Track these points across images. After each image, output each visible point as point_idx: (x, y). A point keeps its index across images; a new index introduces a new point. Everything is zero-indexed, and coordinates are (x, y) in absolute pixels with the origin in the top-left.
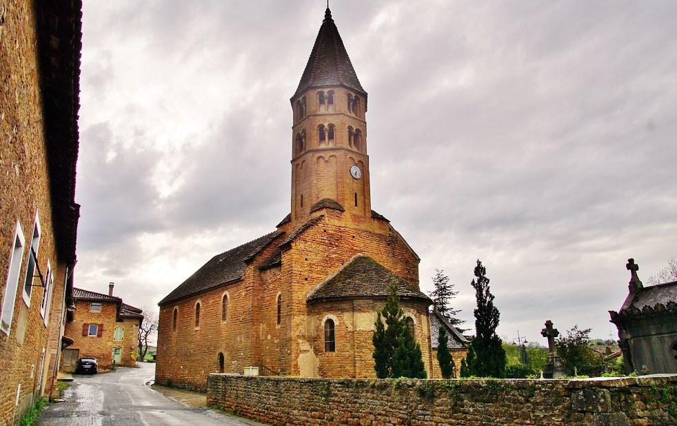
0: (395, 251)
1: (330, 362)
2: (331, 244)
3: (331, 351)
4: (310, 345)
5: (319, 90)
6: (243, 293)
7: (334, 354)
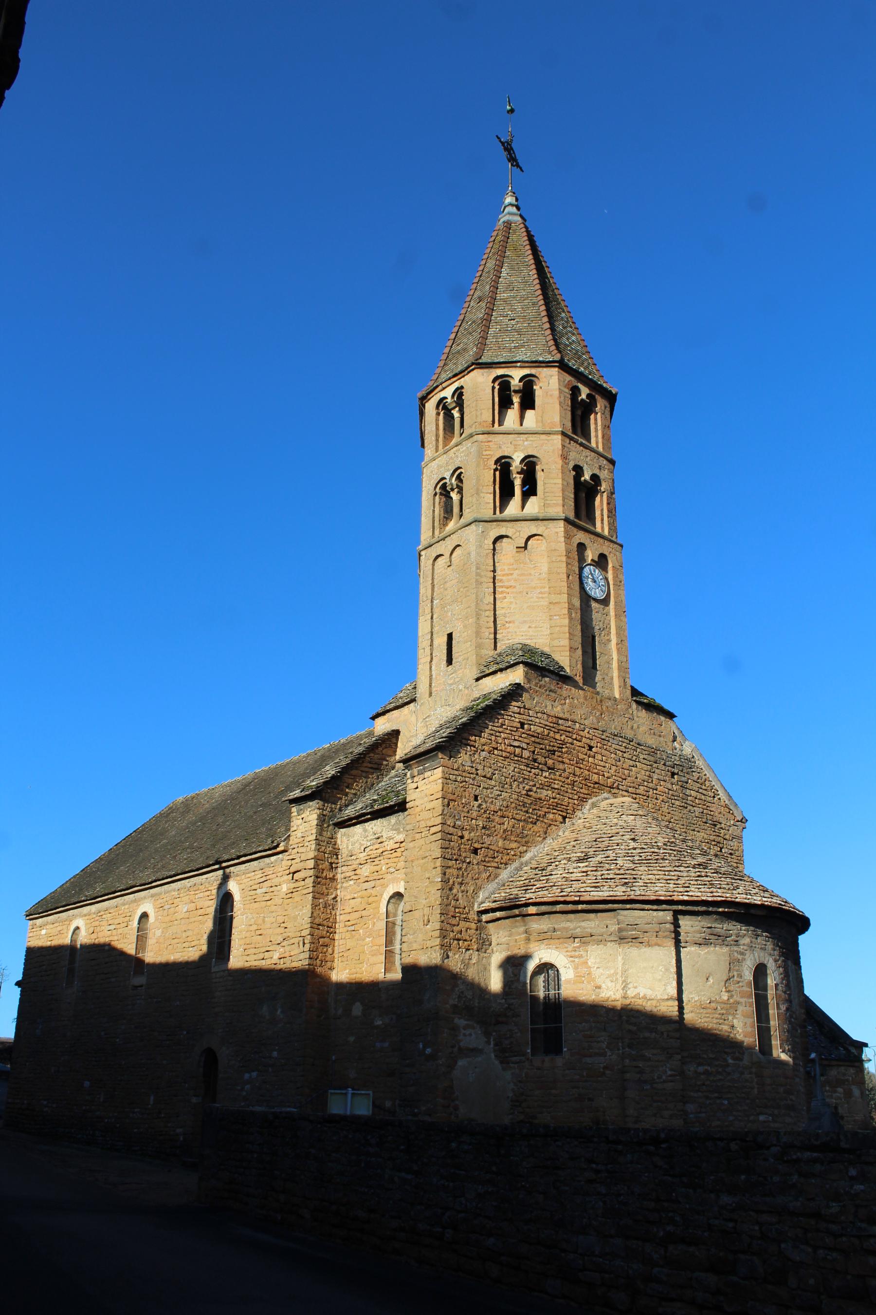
0: (688, 792)
2: (535, 760)
3: (547, 1052)
4: (487, 1034)
5: (500, 372)
6: (285, 888)
7: (559, 1061)
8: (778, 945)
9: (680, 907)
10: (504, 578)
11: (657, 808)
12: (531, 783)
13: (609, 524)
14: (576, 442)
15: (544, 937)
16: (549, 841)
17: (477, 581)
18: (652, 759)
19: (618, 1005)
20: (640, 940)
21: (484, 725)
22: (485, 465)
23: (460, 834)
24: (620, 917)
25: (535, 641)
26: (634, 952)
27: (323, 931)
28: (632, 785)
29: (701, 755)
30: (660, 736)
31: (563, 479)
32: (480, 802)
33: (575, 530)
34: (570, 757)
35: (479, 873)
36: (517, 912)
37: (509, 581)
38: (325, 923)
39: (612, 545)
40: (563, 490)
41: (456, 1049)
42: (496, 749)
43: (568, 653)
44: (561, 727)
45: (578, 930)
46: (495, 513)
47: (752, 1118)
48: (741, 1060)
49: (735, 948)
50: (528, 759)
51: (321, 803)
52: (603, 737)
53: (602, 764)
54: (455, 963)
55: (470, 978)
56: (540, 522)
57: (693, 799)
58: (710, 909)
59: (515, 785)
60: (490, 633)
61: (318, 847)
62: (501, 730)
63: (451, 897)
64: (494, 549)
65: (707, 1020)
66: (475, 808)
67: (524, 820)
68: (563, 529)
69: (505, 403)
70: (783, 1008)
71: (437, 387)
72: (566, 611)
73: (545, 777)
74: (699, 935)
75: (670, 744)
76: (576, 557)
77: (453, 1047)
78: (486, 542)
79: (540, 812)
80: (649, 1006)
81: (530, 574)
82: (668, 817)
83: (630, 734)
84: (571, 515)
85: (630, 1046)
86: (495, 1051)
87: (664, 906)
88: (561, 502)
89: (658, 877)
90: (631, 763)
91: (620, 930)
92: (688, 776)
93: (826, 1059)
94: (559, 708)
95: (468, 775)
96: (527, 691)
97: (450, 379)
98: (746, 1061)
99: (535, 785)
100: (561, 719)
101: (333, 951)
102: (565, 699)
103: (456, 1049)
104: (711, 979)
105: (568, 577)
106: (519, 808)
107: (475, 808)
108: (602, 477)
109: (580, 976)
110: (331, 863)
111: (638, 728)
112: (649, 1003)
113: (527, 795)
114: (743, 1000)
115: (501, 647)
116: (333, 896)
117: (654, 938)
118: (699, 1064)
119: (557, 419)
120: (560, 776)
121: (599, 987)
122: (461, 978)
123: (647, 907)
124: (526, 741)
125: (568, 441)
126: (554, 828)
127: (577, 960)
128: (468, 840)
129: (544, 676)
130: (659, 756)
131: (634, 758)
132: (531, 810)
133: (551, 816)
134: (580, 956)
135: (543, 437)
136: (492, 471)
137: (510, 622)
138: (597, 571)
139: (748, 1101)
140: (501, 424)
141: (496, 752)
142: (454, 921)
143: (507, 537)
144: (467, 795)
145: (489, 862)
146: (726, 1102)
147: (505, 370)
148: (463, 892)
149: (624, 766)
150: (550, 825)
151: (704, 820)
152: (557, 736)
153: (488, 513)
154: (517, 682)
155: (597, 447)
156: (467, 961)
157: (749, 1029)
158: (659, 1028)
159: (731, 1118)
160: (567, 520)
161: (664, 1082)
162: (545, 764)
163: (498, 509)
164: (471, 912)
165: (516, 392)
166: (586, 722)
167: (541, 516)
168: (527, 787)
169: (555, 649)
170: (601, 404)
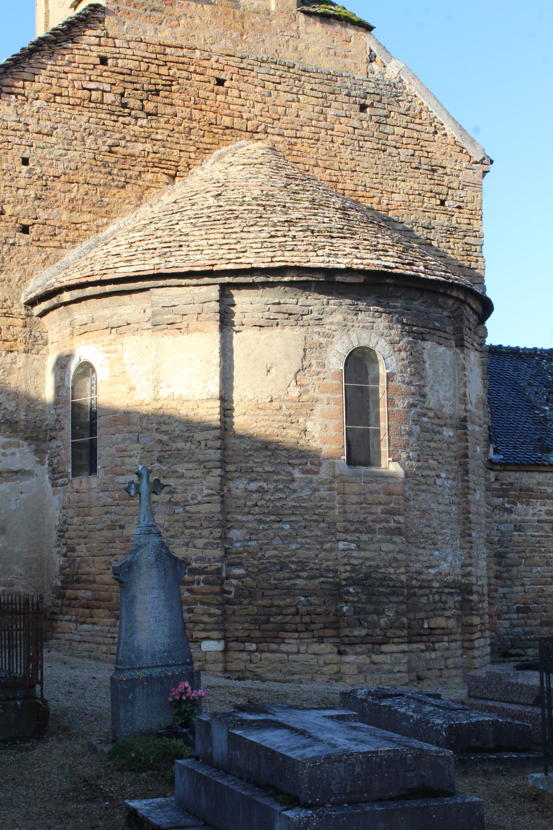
0: (389, 129)
1: (83, 510)
2: (124, 106)
7: (94, 481)
9: (227, 280)
11: (333, 154)
12: (118, 136)
16: (143, 209)
18: (327, 89)
19: (150, 408)
21: (39, 65)
24: (155, 298)
26: (170, 342)
28: (290, 126)
29: (415, 77)
30: (346, 57)
32: (31, 165)
35: (29, 256)
36: (54, 301)
42: (60, 95)
44: (169, 58)
45: (115, 318)
47: (327, 546)
49: (316, 329)
52: (242, 66)
53: (240, 101)
55: (12, 386)
57: (397, 138)
59: (89, 140)
62: (67, 69)
66: (23, 174)
67: (105, 184)
70: (401, 404)
73: (141, 127)
74: (260, 315)
75: (363, 67)
79: (122, 174)
80: (185, 411)
82: (351, 165)
83: (289, 57)
85: (159, 461)
86: (49, 472)
87: (206, 280)
89: (210, 242)
90: (290, 97)
91: (154, 314)
92: (390, 108)
94: (166, 32)
95: (13, 133)
96: (113, 13)
98: (324, 473)
99: (124, 138)
100: (169, 46)
102: (178, 19)
104: (273, 371)
106: (95, 169)
107: (23, 174)
109: (115, 376)
111: (307, 48)
113: (110, 152)
114: (324, 396)
118: (251, 480)
120: (167, 122)
121: (132, 389)
123: (184, 281)
124: (109, 80)
126: (154, 191)
127: (112, 355)
128: (11, 216)
131: (295, 90)
132: (115, 171)
133: (149, 176)
134: (116, 351)
139: (322, 525)
141: (58, 99)
144: (10, 157)
145: (45, 241)
146: (287, 527)
149: (277, 102)
150: (148, 187)
151: (414, 165)
152: (163, 70)
154: (101, 3)
156: (8, 366)
157: (332, 433)
158: (196, 436)
159: (294, 547)
161: (199, 503)
162: (142, 109)
166: (214, 48)
168: (110, 142)
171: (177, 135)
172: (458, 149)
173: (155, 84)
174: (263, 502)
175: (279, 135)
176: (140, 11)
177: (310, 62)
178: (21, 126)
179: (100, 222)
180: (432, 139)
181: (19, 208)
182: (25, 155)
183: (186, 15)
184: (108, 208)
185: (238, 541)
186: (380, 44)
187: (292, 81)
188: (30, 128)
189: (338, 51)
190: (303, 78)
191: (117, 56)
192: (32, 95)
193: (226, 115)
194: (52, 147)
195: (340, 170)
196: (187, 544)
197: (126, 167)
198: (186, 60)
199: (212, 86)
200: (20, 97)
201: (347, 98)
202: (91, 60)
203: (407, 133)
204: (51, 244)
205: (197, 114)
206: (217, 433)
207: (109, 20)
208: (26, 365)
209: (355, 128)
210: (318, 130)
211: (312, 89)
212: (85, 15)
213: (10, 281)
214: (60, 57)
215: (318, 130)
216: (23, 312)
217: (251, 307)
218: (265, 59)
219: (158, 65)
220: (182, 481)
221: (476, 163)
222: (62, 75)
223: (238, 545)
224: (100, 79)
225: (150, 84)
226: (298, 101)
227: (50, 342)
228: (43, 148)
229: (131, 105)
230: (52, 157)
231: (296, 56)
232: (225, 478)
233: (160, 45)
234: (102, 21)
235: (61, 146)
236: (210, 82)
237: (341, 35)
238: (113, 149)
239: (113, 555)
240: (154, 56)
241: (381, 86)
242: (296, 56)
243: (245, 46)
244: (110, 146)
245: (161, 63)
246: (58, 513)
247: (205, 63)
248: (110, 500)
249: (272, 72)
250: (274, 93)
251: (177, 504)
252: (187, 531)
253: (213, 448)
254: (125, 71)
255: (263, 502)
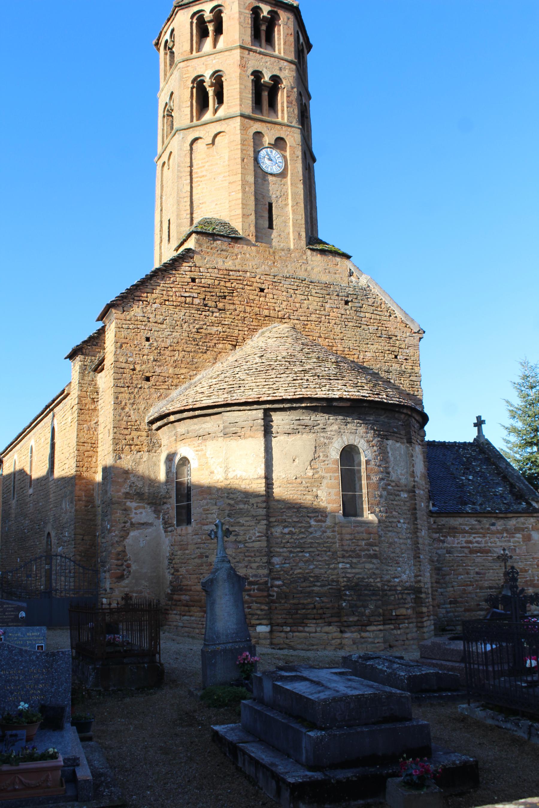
0: (362, 315)
1: (183, 547)
2: (206, 305)
4: (157, 512)
5: (196, 9)
7: (190, 529)
8: (372, 429)
9: (268, 406)
10: (199, 170)
11: (329, 330)
12: (202, 323)
13: (288, 113)
14: (255, 52)
15: (183, 438)
17: (178, 176)
18: (325, 292)
20: (238, 434)
21: (156, 284)
22: (185, 86)
23: (132, 367)
24: (225, 418)
25: (219, 215)
26: (234, 444)
27: (88, 447)
28: (303, 314)
30: (335, 273)
31: (240, 84)
32: (151, 341)
33: (251, 122)
34: (240, 299)
35: (150, 395)
36: (165, 421)
37: (202, 172)
38: (89, 441)
39: (289, 129)
40: (241, 93)
41: (128, 524)
42: (168, 300)
43: (241, 220)
44: (232, 277)
45: (202, 430)
46: (192, 121)
47: (332, 566)
48: (325, 522)
49: (322, 434)
50: (198, 305)
51: (82, 357)
52: (274, 280)
53: (273, 301)
54: (127, 462)
55: (140, 472)
56: (223, 122)
57: (368, 319)
58: (294, 405)
59: (185, 326)
60: (187, 214)
61: (81, 388)
62: (172, 286)
63: (123, 414)
64: (191, 149)
65: (293, 492)
66: (147, 347)
67: (195, 351)
68: (239, 124)
69: (203, 33)
70: (375, 479)
71: (161, 33)
72: (240, 187)
73: (216, 317)
74: (288, 427)
75: (346, 279)
76: (252, 144)
77: (125, 523)
78: (185, 145)
79: (203, 346)
80: (244, 486)
81: (217, 164)
82: (341, 336)
83: (302, 274)
84: (248, 111)
85: (229, 516)
86: (163, 524)
87: (255, 407)
88: (238, 102)
89: (257, 384)
91: (225, 428)
92: (362, 302)
93: (500, 513)
94: (230, 263)
96: (198, 253)
97: (166, 24)
98: (329, 522)
99: (206, 324)
100: (232, 271)
101: (97, 460)
103: (128, 524)
104: (297, 460)
105: (243, 160)
106: (189, 342)
108: (282, 76)
110: (93, 399)
111: (312, 269)
112: (244, 481)
113: (198, 332)
114: (328, 475)
115: (195, 222)
116: (95, 422)
117: (249, 432)
118: (285, 527)
119: (237, 36)
120: (231, 314)
121: (212, 473)
122: (132, 473)
124: (196, 291)
125: (247, 52)
126: (223, 354)
127: (200, 453)
128: (139, 371)
129: (215, 240)
130: (332, 289)
131: (306, 293)
132: (201, 343)
133: (221, 346)
134: (202, 450)
135: (227, 53)
136: (190, 89)
137: (203, 203)
138: (274, 152)
139: (328, 553)
140: (199, 50)
141: (167, 303)
142: (126, 432)
143: (201, 138)
145: (159, 385)
146: (307, 555)
147: (200, 6)
148: (134, 410)
150: (220, 352)
151: (378, 335)
152: (228, 284)
153: (187, 122)
155: (280, 53)
156: (138, 460)
158: (251, 500)
159: (311, 567)
160: (243, 116)
161: (253, 541)
163: (195, 118)
164: (142, 424)
165: (210, 22)
166: (258, 271)
167: (228, 115)
168: (197, 326)
169: (232, 218)
170: (284, 16)
171: (237, 321)
172: (404, 325)
173: (224, 293)
174: (292, 540)
175: (297, 320)
176: (215, 251)
177: (314, 277)
178: (145, 319)
179: (191, 373)
180: (388, 320)
181: (144, 366)
182: (148, 336)
183: (241, 253)
184: (196, 365)
185: (278, 564)
186: (355, 266)
187: (304, 288)
188: (150, 320)
189: (331, 270)
190: (311, 287)
191: (201, 277)
192: (152, 301)
193: (266, 309)
194: (163, 330)
195: (334, 339)
196: (246, 567)
197: (207, 341)
198: (241, 278)
199: (257, 292)
200: (144, 302)
201: (337, 297)
202: (186, 280)
203: (373, 316)
204: (163, 387)
205: (248, 309)
206: (264, 499)
207: (196, 257)
208: (148, 459)
209: (342, 315)
210: (320, 316)
211: (316, 293)
212: (183, 255)
213: (139, 409)
214: (168, 279)
215: (320, 316)
216: (147, 427)
217: (283, 422)
218: (288, 276)
219: (225, 282)
220: (243, 528)
221: (415, 333)
222: (169, 289)
223: (278, 566)
224: (191, 290)
225: (221, 292)
226: (308, 300)
227: (162, 445)
228: (158, 331)
229: (209, 305)
230: (164, 336)
231: (306, 274)
232: (269, 526)
233: (226, 270)
234: (192, 258)
235: (169, 330)
236: (255, 290)
237: (332, 261)
238: (199, 330)
239: (202, 574)
240: (223, 276)
241: (357, 290)
242: (306, 274)
243: (276, 269)
244: (197, 329)
245: (227, 280)
246: (168, 549)
247: (253, 279)
248: (199, 540)
249: (292, 283)
250: (294, 296)
251: (240, 542)
252: (246, 559)
253: (261, 508)
254: (206, 285)
255: (292, 540)
